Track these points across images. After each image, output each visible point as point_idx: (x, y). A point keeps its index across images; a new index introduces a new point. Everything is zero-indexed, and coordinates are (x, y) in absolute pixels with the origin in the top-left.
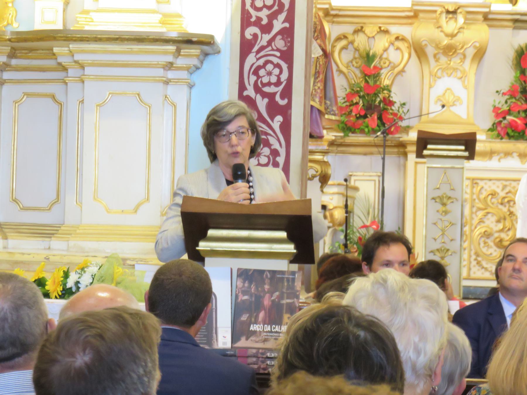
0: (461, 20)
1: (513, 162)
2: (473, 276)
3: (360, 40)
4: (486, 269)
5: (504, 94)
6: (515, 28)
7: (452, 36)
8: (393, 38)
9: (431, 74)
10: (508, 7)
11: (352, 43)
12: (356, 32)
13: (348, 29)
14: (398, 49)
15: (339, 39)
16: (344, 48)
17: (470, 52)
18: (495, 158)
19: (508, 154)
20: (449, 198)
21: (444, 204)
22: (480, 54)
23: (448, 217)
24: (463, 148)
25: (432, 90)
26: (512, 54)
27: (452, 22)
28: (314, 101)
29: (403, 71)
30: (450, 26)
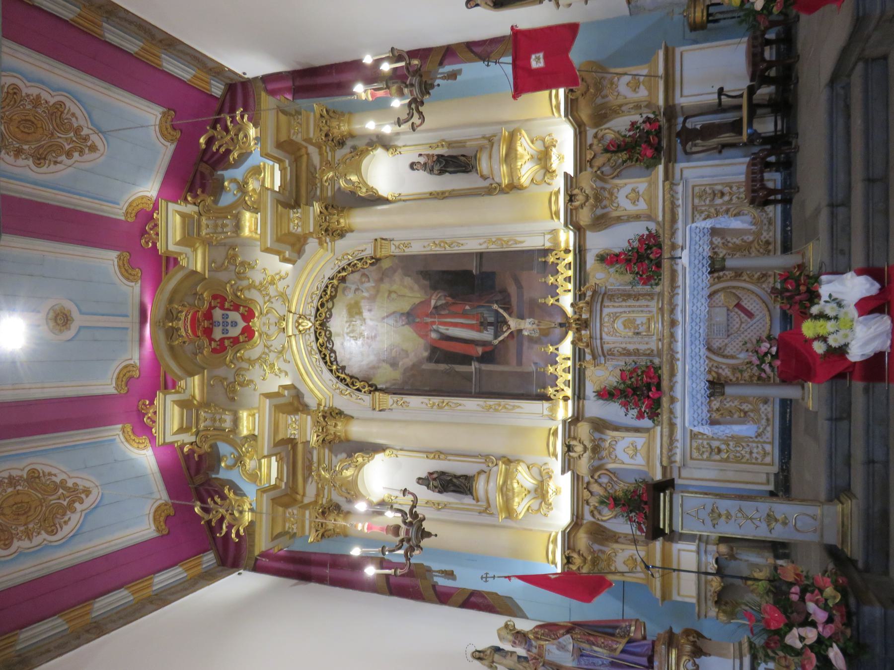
0: (573, 443)
1: (678, 406)
2: (770, 440)
3: (594, 501)
4: (765, 429)
5: (627, 409)
6: (584, 399)
7: (585, 449)
8: (592, 480)
9: (614, 462)
10: (570, 402)
11: (596, 508)
12: (588, 503)
13: (587, 509)
14: (599, 477)
15: (593, 516)
16: (600, 513)
17: (597, 435)
18: (674, 421)
19: (671, 412)
20: (713, 511)
21: (720, 515)
22: (600, 426)
23: (733, 513)
24: (662, 494)
25: (625, 461)
26: (601, 402)
27: (576, 449)
28: (615, 649)
29: (614, 474)
30: (579, 448)
